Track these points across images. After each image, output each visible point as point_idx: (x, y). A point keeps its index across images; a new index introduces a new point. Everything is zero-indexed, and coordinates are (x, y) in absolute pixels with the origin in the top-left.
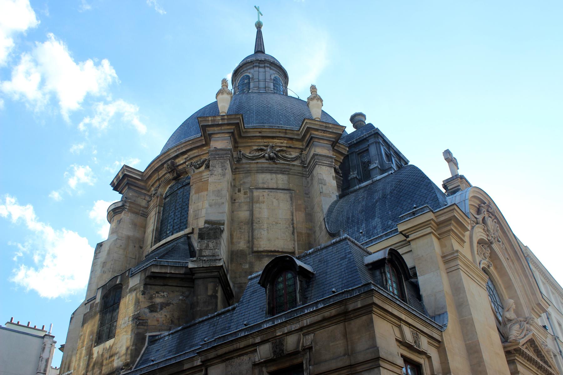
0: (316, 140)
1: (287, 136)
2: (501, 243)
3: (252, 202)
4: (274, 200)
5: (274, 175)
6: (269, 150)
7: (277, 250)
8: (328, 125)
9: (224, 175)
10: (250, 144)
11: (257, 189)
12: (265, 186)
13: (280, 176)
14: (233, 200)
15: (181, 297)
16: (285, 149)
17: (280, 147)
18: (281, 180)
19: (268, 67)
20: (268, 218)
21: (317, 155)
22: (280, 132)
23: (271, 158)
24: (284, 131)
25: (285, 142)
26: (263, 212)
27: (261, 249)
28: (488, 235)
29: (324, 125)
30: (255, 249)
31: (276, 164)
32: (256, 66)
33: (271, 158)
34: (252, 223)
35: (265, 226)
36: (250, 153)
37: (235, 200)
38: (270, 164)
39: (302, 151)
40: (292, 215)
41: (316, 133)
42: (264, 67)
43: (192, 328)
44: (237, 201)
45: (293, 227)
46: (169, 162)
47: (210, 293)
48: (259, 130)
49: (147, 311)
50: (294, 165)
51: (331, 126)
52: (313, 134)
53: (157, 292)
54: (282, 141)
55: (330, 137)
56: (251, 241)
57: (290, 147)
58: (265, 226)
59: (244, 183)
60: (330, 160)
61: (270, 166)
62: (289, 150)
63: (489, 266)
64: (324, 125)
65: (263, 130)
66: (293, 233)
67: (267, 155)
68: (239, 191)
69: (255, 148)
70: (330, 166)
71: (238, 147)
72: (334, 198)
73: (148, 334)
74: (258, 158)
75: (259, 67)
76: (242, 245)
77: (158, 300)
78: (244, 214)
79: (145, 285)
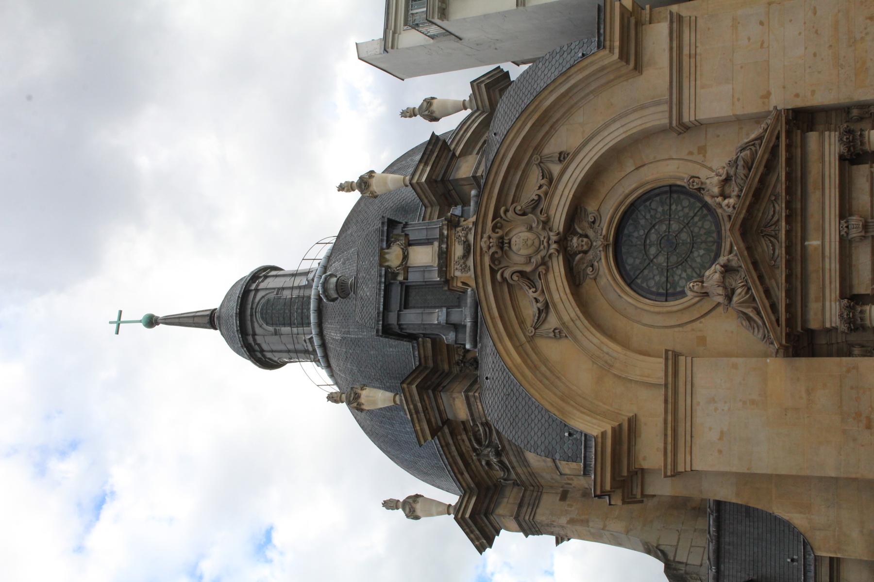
0: (444, 416)
1: (451, 442)
8: (413, 411)
10: (485, 476)
16: (470, 434)
17: (470, 440)
22: (450, 453)
24: (445, 448)
25: (459, 437)
28: (550, 256)
29: (415, 416)
38: (507, 454)
48: (459, 476)
51: (412, 407)
52: (436, 423)
54: (461, 443)
55: (429, 397)
60: (472, 399)
61: (511, 453)
62: (469, 428)
64: (415, 416)
65: (456, 471)
68: (570, 484)
71: (495, 486)
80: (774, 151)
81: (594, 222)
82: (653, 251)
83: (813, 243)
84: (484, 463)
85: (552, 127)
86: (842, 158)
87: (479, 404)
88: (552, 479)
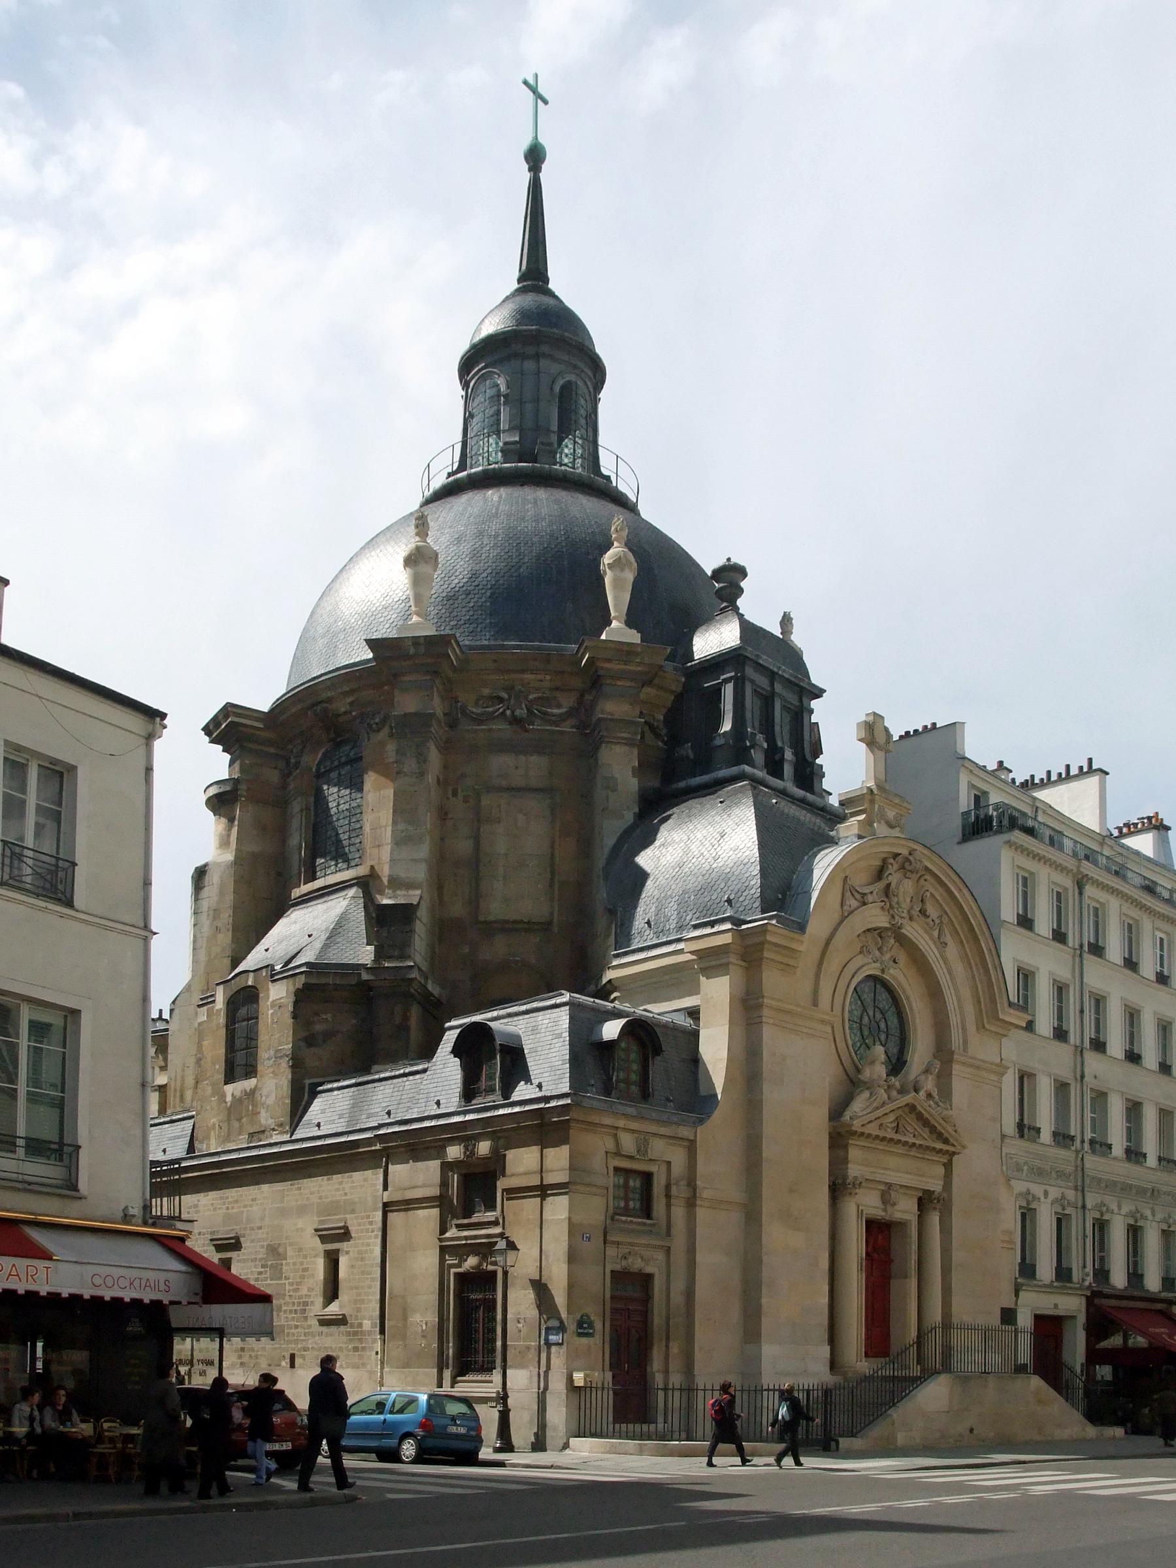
2: (929, 920)
3: (479, 819)
4: (520, 816)
5: (522, 758)
6: (512, 702)
7: (519, 918)
9: (421, 774)
11: (490, 789)
12: (504, 783)
13: (534, 759)
14: (443, 814)
15: (354, 1021)
16: (548, 694)
18: (534, 768)
19: (545, 356)
20: (506, 855)
21: (604, 719)
23: (516, 721)
25: (548, 677)
26: (499, 842)
27: (492, 918)
30: (481, 918)
31: (527, 731)
32: (516, 355)
33: (516, 721)
34: (477, 866)
35: (501, 870)
36: (476, 704)
37: (446, 814)
39: (582, 695)
40: (552, 847)
41: (607, 665)
42: (537, 356)
43: (370, 1086)
44: (450, 816)
45: (552, 873)
46: (319, 708)
47: (398, 1020)
49: (302, 1044)
50: (562, 733)
53: (317, 1014)
54: (539, 677)
56: (475, 900)
57: (557, 689)
58: (501, 870)
59: (463, 775)
62: (558, 694)
63: (883, 971)
66: (551, 885)
67: (508, 712)
68: (455, 794)
69: (486, 692)
70: (629, 743)
72: (629, 817)
73: (307, 1082)
74: (490, 717)
75: (524, 357)
76: (457, 909)
77: (319, 1028)
78: (463, 846)
79: (296, 1003)
80: (946, 1141)
81: (895, 961)
82: (878, 1016)
83: (892, 1161)
84: (505, 696)
85: (962, 942)
86: (926, 1192)
87: (625, 735)
88: (463, 775)
